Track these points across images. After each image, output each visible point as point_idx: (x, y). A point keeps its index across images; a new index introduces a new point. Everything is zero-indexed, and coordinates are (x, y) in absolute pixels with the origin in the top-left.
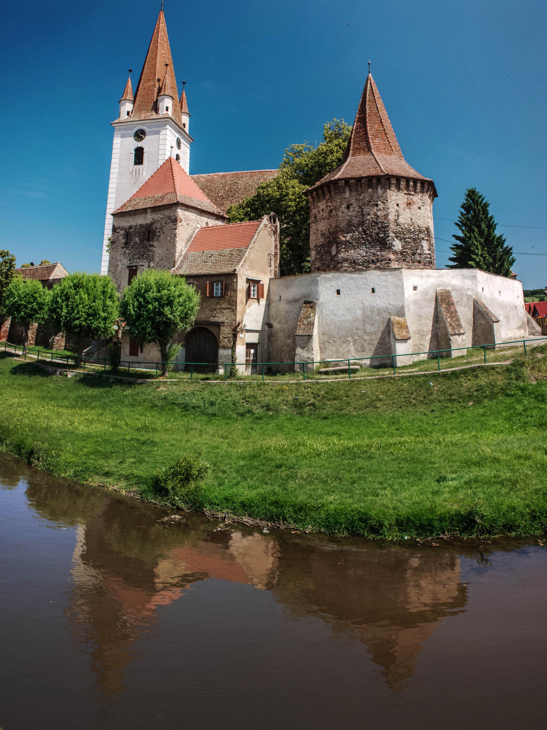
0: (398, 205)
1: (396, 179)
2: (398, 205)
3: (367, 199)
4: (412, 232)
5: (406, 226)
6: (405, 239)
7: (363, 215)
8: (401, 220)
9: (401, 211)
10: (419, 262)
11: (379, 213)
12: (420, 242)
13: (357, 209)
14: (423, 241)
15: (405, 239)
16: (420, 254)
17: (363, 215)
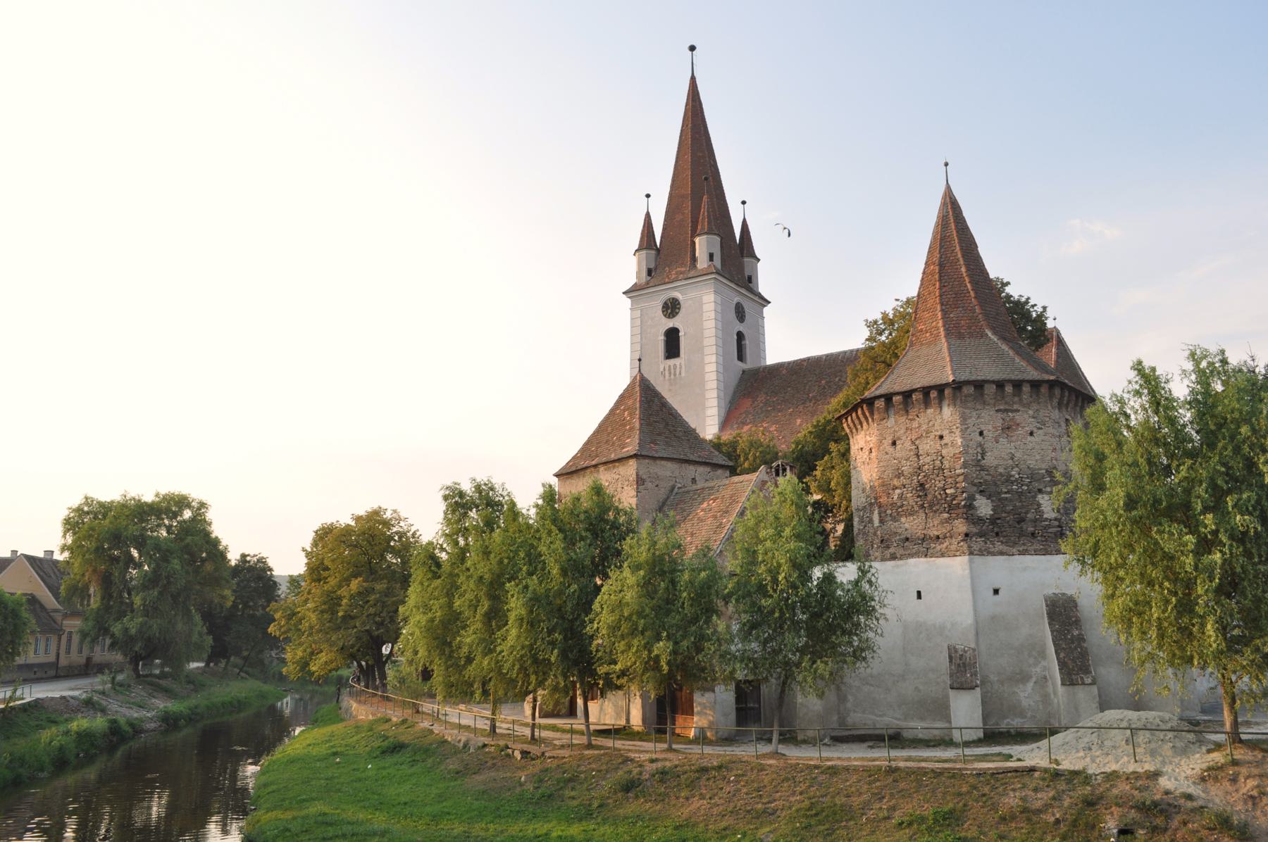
0: (981, 433)
1: (976, 387)
2: (981, 433)
3: (924, 427)
4: (1016, 480)
5: (1001, 470)
6: (999, 493)
7: (918, 456)
8: (990, 460)
9: (988, 445)
10: (1033, 534)
11: (944, 452)
12: (1035, 497)
13: (908, 444)
14: (1040, 496)
15: (999, 493)
16: (1035, 521)
17: (918, 456)
